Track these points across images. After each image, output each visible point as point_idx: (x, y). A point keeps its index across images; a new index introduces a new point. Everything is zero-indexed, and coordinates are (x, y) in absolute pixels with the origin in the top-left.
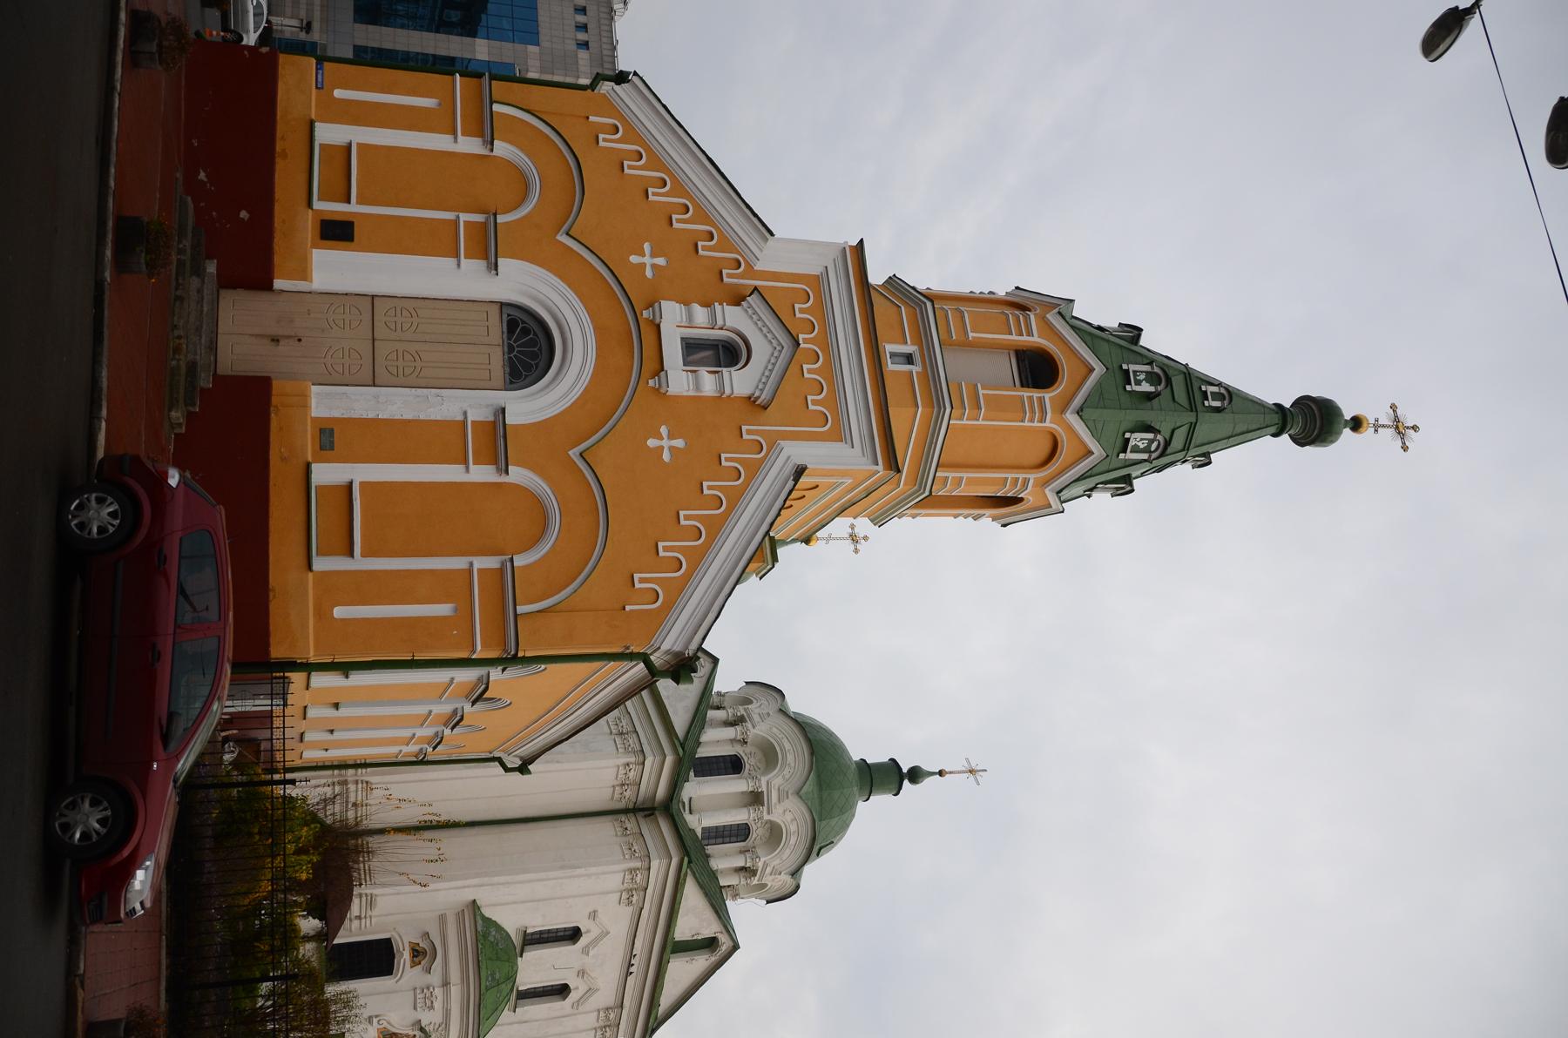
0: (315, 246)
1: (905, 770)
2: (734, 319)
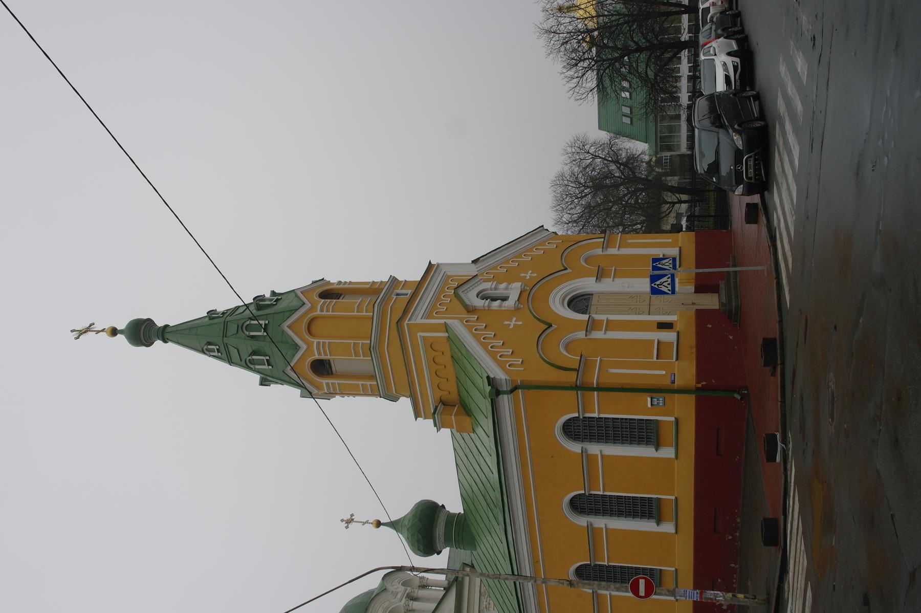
0: (676, 322)
2: (479, 303)
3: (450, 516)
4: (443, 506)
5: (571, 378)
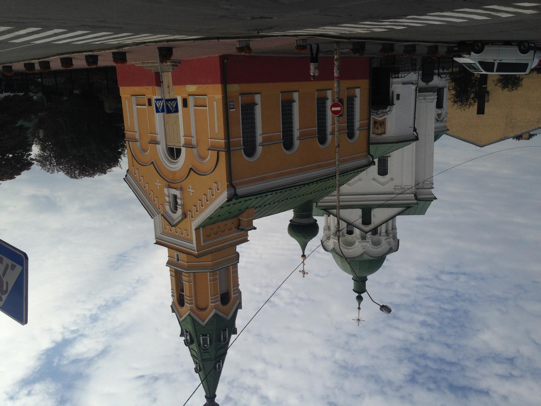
1: (362, 295)
3: (296, 216)
4: (291, 221)
5: (223, 155)
